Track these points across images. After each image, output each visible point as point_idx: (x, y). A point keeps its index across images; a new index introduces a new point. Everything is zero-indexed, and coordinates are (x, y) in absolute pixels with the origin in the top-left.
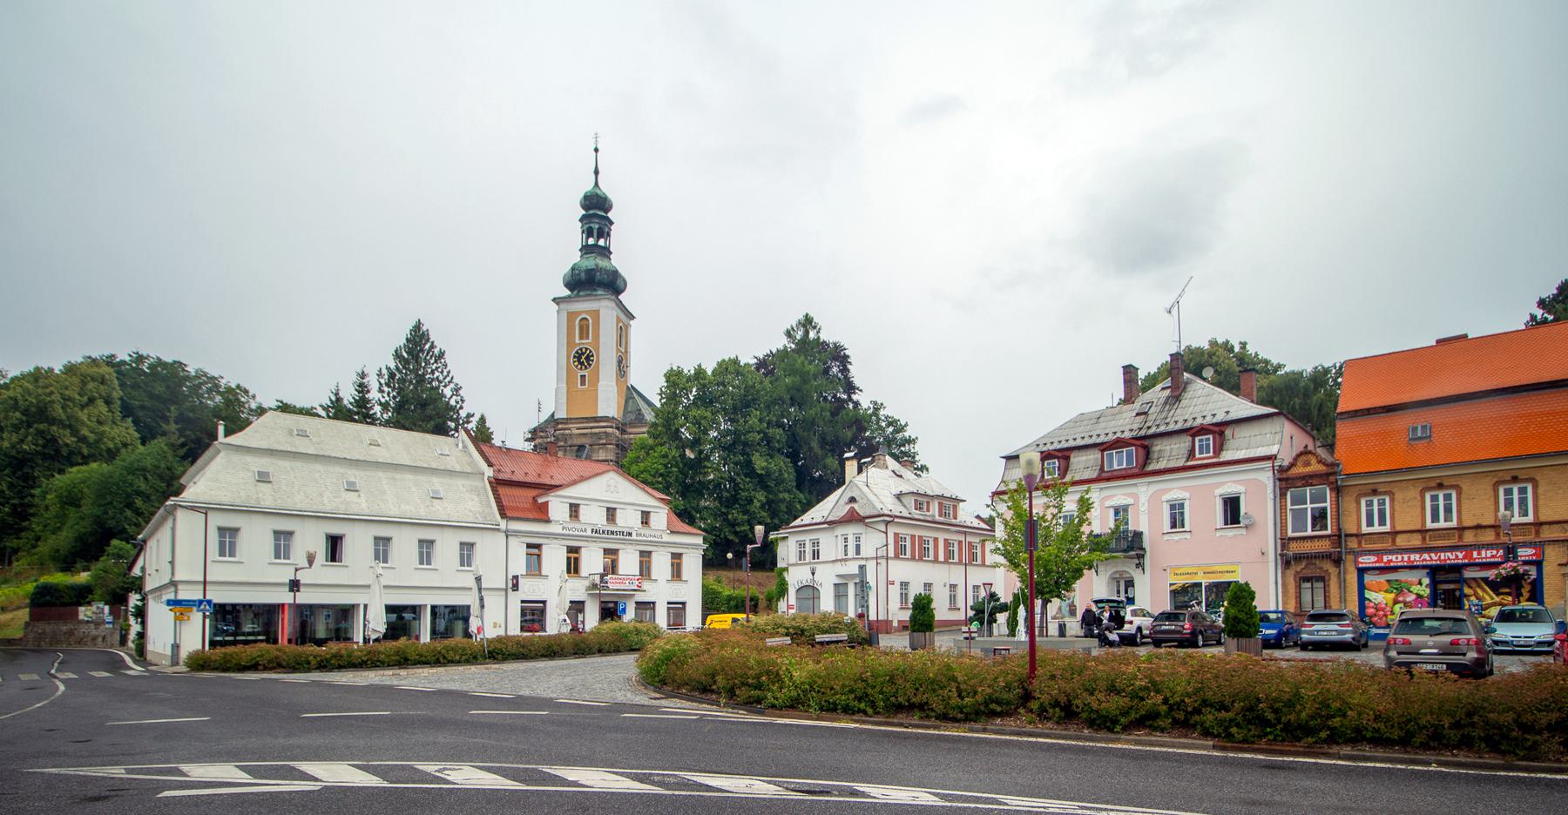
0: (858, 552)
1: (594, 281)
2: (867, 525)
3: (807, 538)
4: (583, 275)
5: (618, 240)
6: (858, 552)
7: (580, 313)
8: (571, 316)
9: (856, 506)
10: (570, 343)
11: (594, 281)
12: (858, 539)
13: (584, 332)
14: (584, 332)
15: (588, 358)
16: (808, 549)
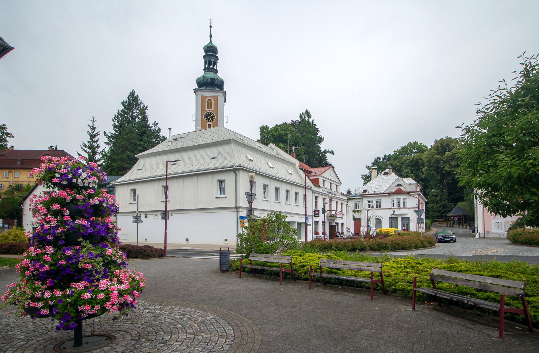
0: (404, 205)
1: (210, 83)
2: (411, 195)
3: (374, 200)
4: (209, 81)
5: (220, 66)
6: (404, 205)
7: (208, 97)
8: (203, 98)
9: (401, 188)
10: (203, 110)
11: (210, 83)
12: (404, 200)
13: (210, 105)
14: (210, 105)
15: (212, 117)
16: (374, 203)
